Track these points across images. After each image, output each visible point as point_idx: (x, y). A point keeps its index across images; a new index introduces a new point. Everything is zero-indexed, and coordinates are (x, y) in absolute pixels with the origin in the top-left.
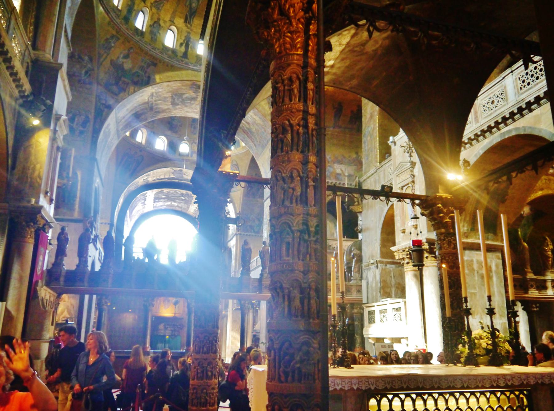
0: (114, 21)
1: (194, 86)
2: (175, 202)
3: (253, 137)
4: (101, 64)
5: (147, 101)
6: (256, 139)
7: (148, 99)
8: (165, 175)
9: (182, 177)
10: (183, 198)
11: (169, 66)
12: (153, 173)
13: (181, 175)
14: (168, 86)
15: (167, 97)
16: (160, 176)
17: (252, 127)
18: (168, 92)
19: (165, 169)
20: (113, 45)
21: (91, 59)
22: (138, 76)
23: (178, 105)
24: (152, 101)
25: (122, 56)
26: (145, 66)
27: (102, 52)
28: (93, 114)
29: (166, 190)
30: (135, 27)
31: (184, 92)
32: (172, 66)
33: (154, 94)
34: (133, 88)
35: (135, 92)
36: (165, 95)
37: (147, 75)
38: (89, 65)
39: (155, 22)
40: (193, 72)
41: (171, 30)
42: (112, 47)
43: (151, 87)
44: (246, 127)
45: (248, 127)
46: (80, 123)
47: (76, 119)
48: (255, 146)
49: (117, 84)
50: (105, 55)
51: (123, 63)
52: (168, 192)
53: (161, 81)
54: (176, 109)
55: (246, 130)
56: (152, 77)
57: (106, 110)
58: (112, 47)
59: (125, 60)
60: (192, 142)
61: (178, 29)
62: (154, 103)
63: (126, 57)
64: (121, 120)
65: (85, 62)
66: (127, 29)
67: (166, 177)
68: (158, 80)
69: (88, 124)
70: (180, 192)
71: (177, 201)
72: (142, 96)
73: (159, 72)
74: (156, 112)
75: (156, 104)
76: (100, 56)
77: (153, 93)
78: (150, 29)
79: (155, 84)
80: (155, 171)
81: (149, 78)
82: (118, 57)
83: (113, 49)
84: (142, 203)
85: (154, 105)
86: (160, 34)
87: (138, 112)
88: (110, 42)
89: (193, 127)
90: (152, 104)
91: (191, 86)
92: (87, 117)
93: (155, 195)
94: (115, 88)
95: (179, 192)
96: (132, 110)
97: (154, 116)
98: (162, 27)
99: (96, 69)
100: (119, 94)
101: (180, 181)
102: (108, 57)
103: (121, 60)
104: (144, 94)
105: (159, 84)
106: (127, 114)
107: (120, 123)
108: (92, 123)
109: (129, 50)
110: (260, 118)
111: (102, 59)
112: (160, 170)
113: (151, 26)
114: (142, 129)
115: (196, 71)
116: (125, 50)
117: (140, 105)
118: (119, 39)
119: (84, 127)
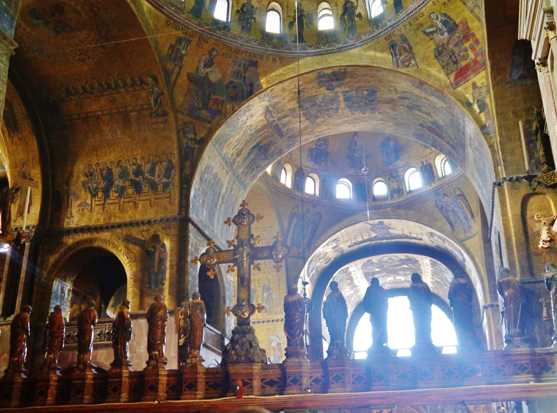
0: (175, 18)
1: (323, 79)
2: (399, 275)
3: (444, 135)
4: (175, 81)
5: (266, 122)
6: (450, 136)
7: (268, 121)
8: (362, 235)
9: (389, 233)
10: (405, 266)
11: (277, 59)
12: (342, 235)
13: (385, 231)
14: (283, 90)
15: (294, 109)
16: (355, 238)
17: (436, 118)
18: (289, 101)
19: (358, 226)
20: (183, 52)
21: (155, 80)
22: (235, 87)
23: (317, 117)
24: (274, 121)
25: (202, 65)
26: (241, 69)
27: (170, 66)
28: (176, 156)
29: (375, 259)
30: (214, 19)
31: (315, 94)
32: (281, 59)
33: (271, 109)
34: (231, 106)
35: (234, 111)
36: (289, 107)
37: (248, 82)
38: (156, 89)
39: (244, 5)
40: (315, 58)
41: (273, 9)
42: (182, 57)
43: (256, 98)
44: (429, 121)
45: (431, 120)
46: (163, 173)
47: (157, 169)
48: (452, 147)
49: (205, 106)
50: (177, 69)
51: (207, 74)
52: (380, 262)
53: (269, 86)
54: (318, 125)
55: (431, 127)
56: (256, 84)
57: (196, 146)
58: (184, 55)
59: (209, 69)
60: (389, 177)
61: (280, 5)
62: (279, 122)
63: (209, 64)
64: (235, 159)
65: (150, 85)
66: (199, 25)
67: (366, 237)
68: (265, 86)
69: (173, 171)
70: (396, 257)
71: (400, 272)
72: (251, 116)
73: (266, 74)
74: (290, 137)
75: (285, 125)
76: (168, 74)
77: (267, 107)
78: (237, 16)
79: (261, 92)
80: (343, 231)
81: (251, 85)
82: (198, 68)
83: (185, 58)
84: (349, 285)
85: (280, 126)
86: (255, 19)
87: (260, 142)
88: (178, 50)
89: (385, 154)
90: (277, 125)
91: (317, 80)
92: (170, 162)
93: (362, 269)
94: (204, 113)
95: (396, 259)
96: (247, 142)
97: (290, 145)
98: (257, 8)
99: (166, 92)
100: (213, 119)
101: (389, 241)
102: (182, 71)
103: (203, 71)
104: (252, 111)
105: (268, 90)
106: (242, 149)
107: (236, 164)
108: (177, 170)
109: (210, 53)
110: (436, 96)
111: (174, 77)
112: (350, 229)
113: (238, 11)
114: (311, 175)
115: (319, 55)
116: (204, 55)
117: (258, 131)
118: (191, 41)
119: (168, 178)
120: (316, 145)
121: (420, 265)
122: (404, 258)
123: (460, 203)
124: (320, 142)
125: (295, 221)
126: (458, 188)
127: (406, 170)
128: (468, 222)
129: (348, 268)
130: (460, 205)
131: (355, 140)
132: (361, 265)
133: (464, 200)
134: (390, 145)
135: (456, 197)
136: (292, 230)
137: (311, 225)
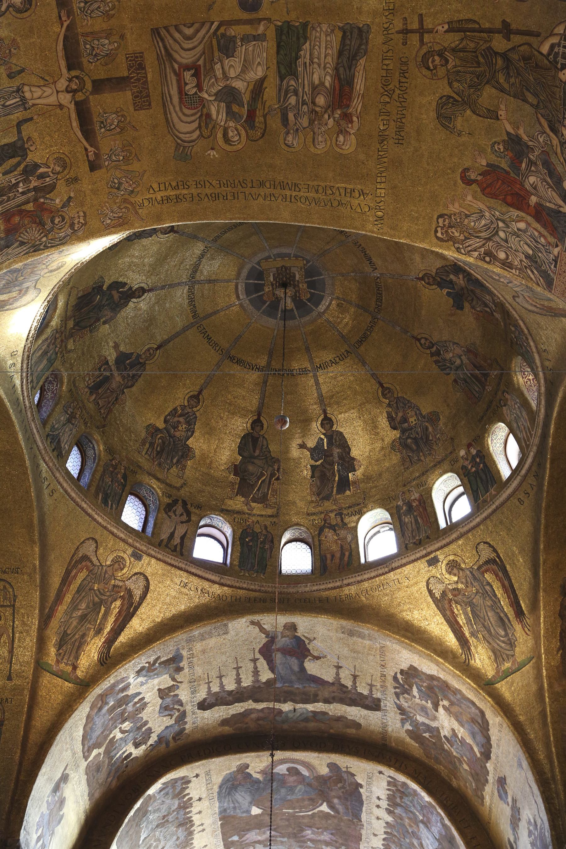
120: (166, 421)
121: (361, 803)
122: (324, 771)
123: (489, 584)
124: (176, 419)
125: (82, 575)
126: (485, 543)
127: (361, 513)
128: (505, 630)
129: (186, 781)
130: (488, 588)
131: (255, 434)
132: (220, 779)
133: (500, 574)
134: (332, 455)
135: (479, 568)
136: (68, 598)
137: (118, 603)
